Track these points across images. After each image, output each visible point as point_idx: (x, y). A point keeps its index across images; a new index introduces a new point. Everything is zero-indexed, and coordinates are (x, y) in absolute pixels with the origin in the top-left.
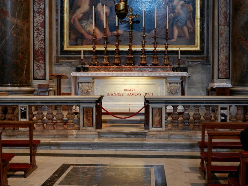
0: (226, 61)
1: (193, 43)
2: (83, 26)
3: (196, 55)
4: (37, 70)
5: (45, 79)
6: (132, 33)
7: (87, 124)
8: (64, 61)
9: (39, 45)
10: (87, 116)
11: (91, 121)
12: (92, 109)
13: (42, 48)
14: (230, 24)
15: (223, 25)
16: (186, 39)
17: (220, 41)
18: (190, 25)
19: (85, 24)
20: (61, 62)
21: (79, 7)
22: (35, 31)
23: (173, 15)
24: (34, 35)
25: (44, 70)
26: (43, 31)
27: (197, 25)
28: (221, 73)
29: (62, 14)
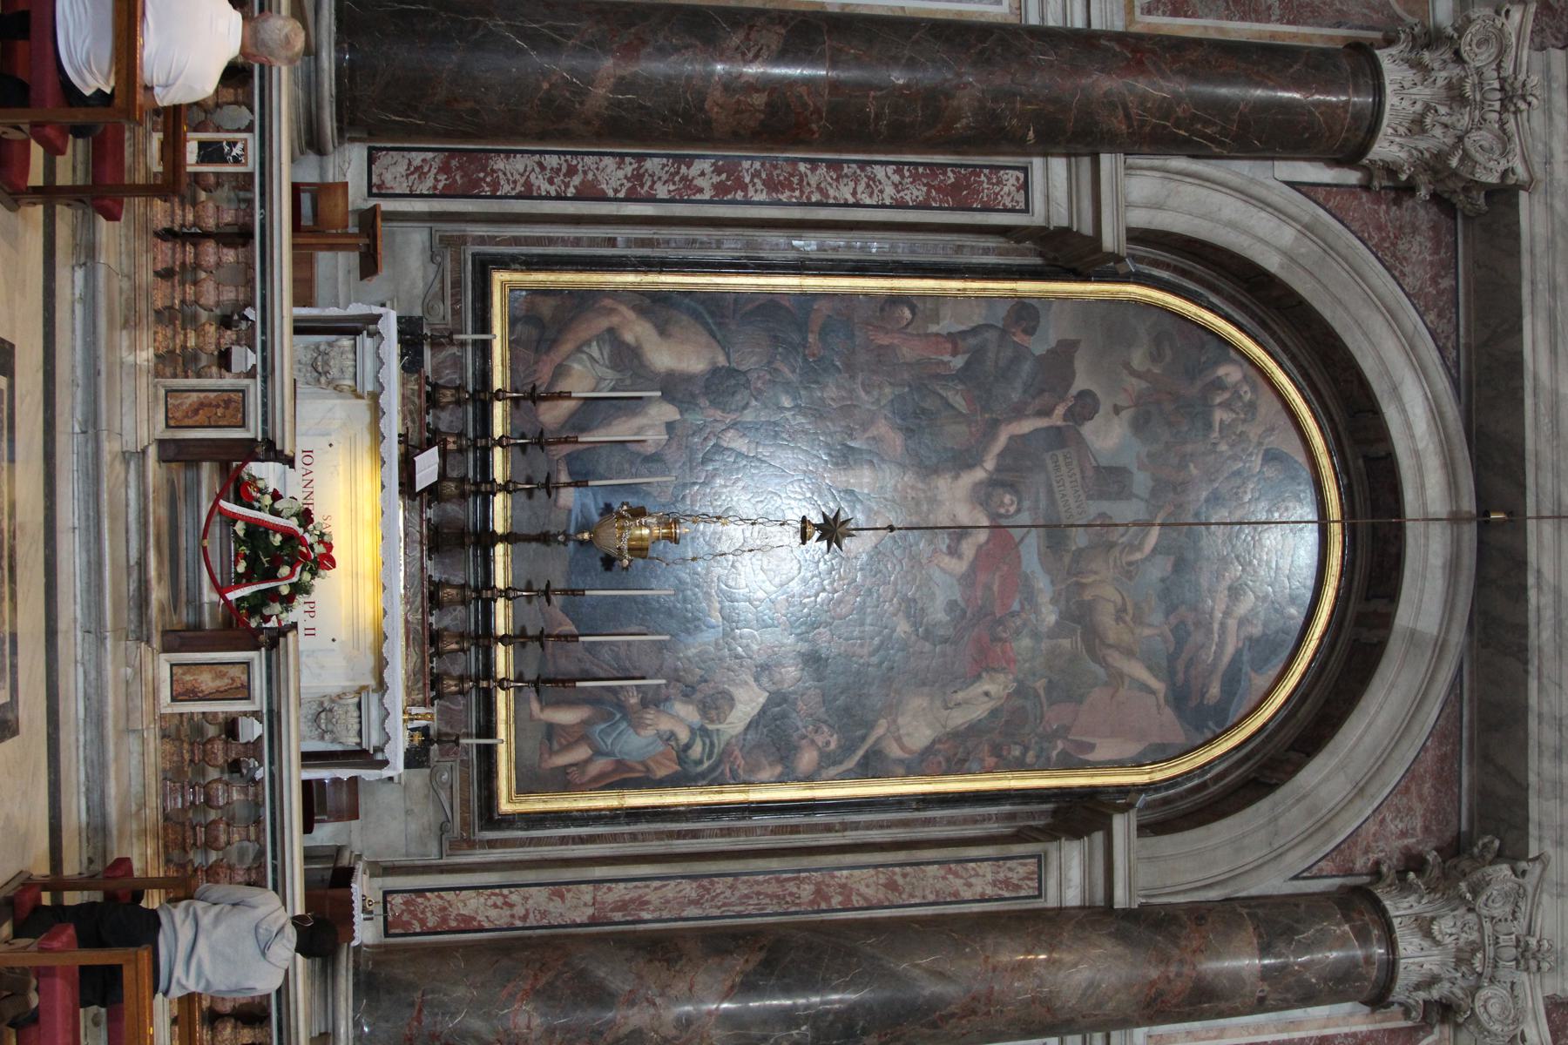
1: (527, 783)
2: (590, 346)
6: (559, 542)
7: (177, 407)
8: (448, 265)
10: (210, 405)
11: (190, 422)
13: (495, 185)
18: (595, 769)
19: (596, 354)
21: (663, 331)
22: (566, 161)
23: (633, 701)
27: (594, 798)
28: (405, 903)
29: (633, 266)
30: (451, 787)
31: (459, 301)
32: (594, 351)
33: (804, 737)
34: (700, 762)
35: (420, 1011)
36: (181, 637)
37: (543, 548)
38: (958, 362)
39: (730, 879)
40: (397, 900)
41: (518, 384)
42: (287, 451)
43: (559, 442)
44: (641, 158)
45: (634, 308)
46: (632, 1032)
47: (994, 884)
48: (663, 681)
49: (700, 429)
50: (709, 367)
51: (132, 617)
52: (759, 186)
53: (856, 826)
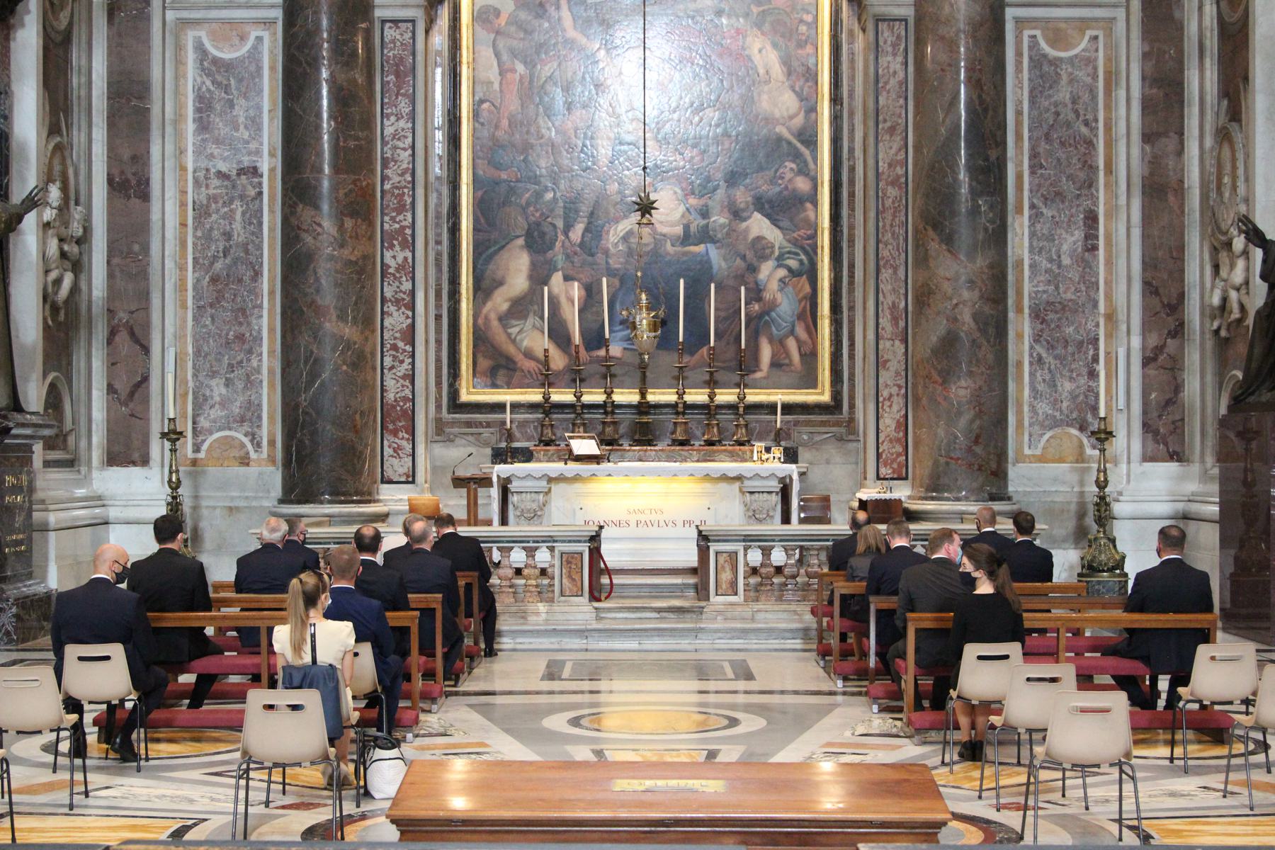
1: (810, 381)
3: (821, 414)
5: (413, 482)
7: (571, 590)
8: (456, 430)
13: (405, 399)
14: (907, 333)
17: (881, 381)
19: (517, 329)
21: (500, 283)
28: (885, 466)
29: (455, 303)
31: (481, 423)
32: (513, 331)
33: (786, 188)
34: (801, 262)
35: (951, 458)
38: (520, 68)
39: (881, 246)
40: (883, 471)
42: (597, 529)
43: (578, 358)
45: (484, 303)
46: (974, 320)
47: (895, 55)
48: (743, 289)
49: (568, 256)
52: (401, 217)
53: (851, 150)
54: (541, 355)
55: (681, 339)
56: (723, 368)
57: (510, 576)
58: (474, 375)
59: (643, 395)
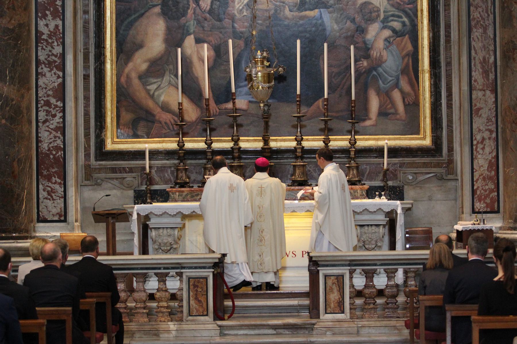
0: (491, 172)
2: (150, 90)
3: (423, 157)
4: (45, 200)
5: (65, 221)
6: (269, 109)
7: (197, 311)
8: (102, 175)
9: (51, 141)
10: (196, 295)
12: (205, 279)
13: (57, 148)
15: (481, 90)
16: (398, 120)
17: (475, 126)
18: (407, 88)
19: (154, 86)
20: (99, 179)
21: (140, 46)
22: (42, 107)
23: (365, 64)
24: (39, 118)
25: (63, 200)
26: (60, 108)
27: (424, 87)
28: (480, 201)
29: (101, 64)
30: (415, 173)
34: (404, 24)
36: (313, 309)
37: (272, 118)
39: (472, 8)
40: (478, 206)
41: (173, 133)
42: (219, 256)
43: (208, 110)
44: (38, 63)
45: (126, 64)
48: (352, 47)
49: (199, 22)
50: (162, 17)
51: (302, 332)
54: (175, 107)
55: (298, 92)
56: (337, 118)
57: (144, 299)
58: (118, 126)
59: (266, 142)
